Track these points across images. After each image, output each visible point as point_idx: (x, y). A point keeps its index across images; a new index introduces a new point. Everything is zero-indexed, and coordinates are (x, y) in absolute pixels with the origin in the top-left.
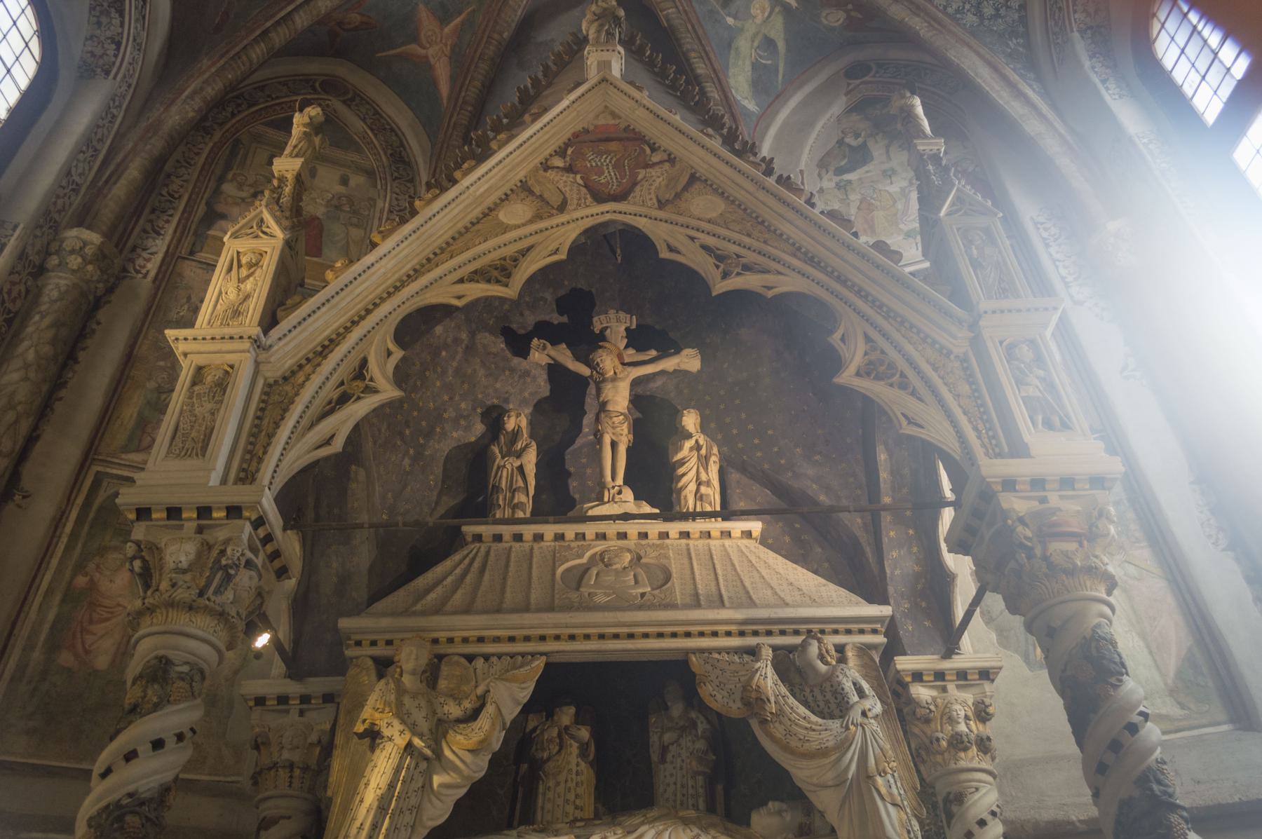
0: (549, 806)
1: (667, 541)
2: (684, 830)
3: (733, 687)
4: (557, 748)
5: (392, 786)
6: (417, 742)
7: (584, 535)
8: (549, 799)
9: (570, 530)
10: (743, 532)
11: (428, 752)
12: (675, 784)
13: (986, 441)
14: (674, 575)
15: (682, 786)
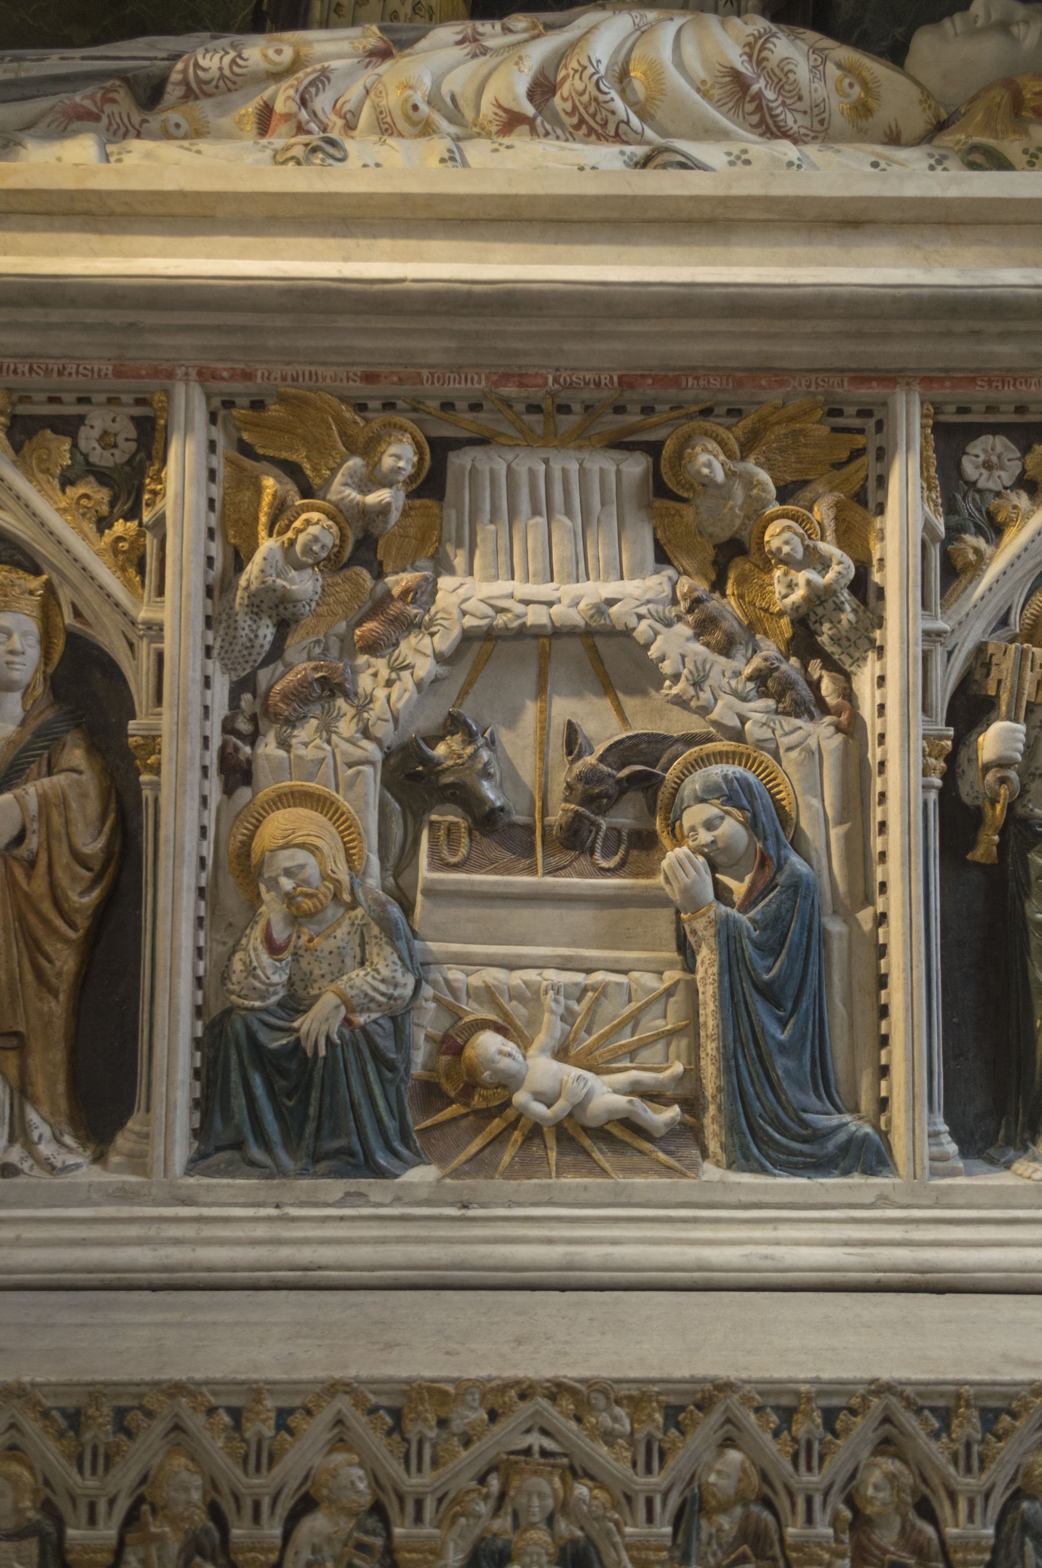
2: (723, 24)
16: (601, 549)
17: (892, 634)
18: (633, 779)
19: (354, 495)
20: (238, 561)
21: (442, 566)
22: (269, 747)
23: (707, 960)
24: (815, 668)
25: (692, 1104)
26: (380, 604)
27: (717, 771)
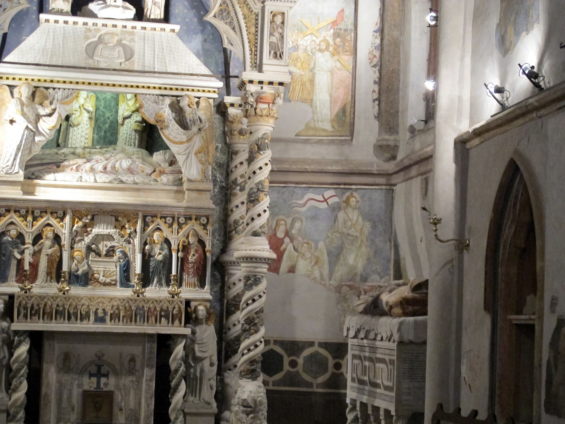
0: (74, 138)
1: (135, 30)
3: (152, 112)
4: (79, 114)
5: (21, 141)
6: (30, 126)
7: (97, 24)
8: (74, 135)
9: (90, 21)
10: (171, 30)
11: (34, 130)
12: (127, 134)
13: (253, 56)
14: (136, 53)
15: (130, 135)
16: (109, 227)
17: (138, 236)
18: (112, 250)
19: (85, 221)
20: (73, 226)
21: (93, 228)
22: (75, 246)
23: (118, 268)
24: (131, 239)
25: (116, 281)
26: (87, 232)
27: (119, 250)
